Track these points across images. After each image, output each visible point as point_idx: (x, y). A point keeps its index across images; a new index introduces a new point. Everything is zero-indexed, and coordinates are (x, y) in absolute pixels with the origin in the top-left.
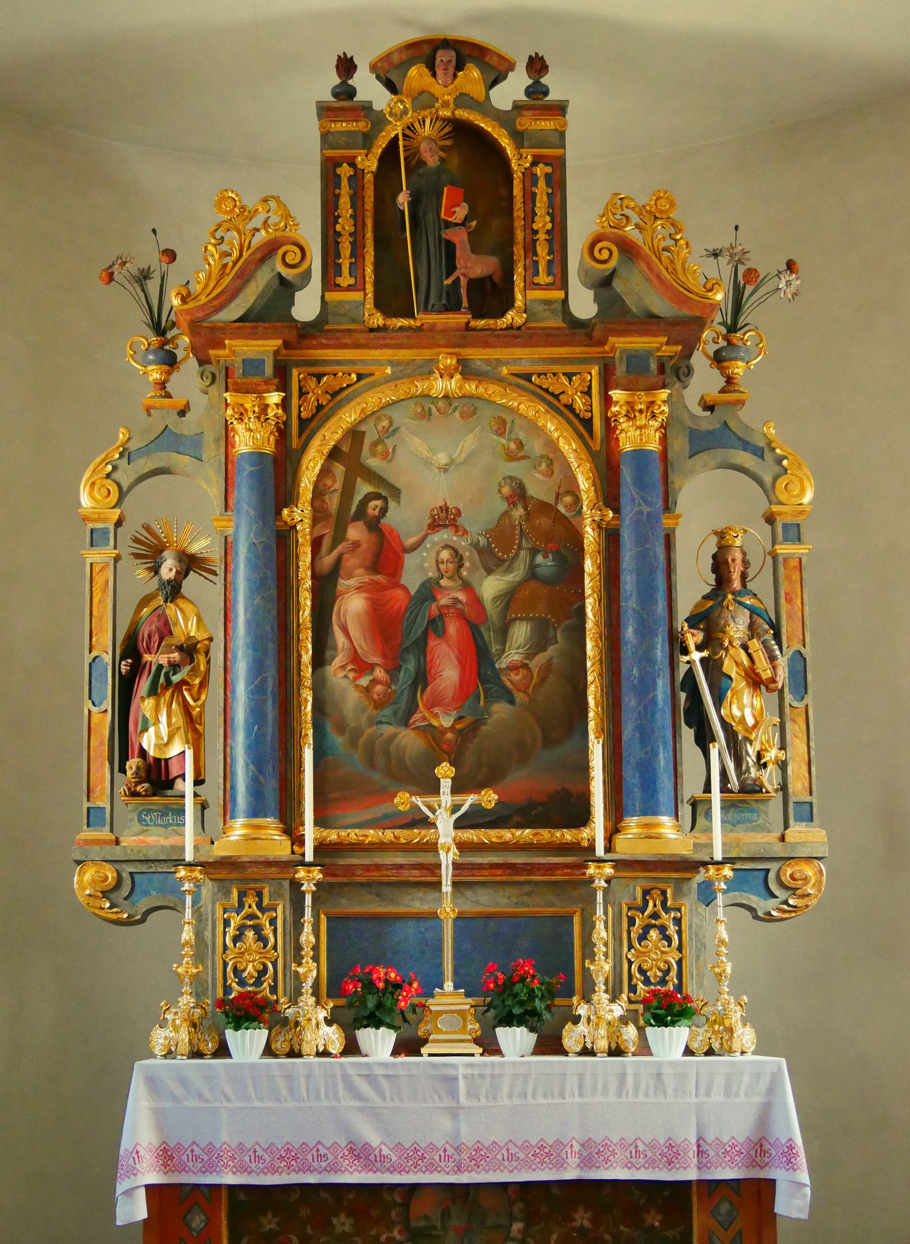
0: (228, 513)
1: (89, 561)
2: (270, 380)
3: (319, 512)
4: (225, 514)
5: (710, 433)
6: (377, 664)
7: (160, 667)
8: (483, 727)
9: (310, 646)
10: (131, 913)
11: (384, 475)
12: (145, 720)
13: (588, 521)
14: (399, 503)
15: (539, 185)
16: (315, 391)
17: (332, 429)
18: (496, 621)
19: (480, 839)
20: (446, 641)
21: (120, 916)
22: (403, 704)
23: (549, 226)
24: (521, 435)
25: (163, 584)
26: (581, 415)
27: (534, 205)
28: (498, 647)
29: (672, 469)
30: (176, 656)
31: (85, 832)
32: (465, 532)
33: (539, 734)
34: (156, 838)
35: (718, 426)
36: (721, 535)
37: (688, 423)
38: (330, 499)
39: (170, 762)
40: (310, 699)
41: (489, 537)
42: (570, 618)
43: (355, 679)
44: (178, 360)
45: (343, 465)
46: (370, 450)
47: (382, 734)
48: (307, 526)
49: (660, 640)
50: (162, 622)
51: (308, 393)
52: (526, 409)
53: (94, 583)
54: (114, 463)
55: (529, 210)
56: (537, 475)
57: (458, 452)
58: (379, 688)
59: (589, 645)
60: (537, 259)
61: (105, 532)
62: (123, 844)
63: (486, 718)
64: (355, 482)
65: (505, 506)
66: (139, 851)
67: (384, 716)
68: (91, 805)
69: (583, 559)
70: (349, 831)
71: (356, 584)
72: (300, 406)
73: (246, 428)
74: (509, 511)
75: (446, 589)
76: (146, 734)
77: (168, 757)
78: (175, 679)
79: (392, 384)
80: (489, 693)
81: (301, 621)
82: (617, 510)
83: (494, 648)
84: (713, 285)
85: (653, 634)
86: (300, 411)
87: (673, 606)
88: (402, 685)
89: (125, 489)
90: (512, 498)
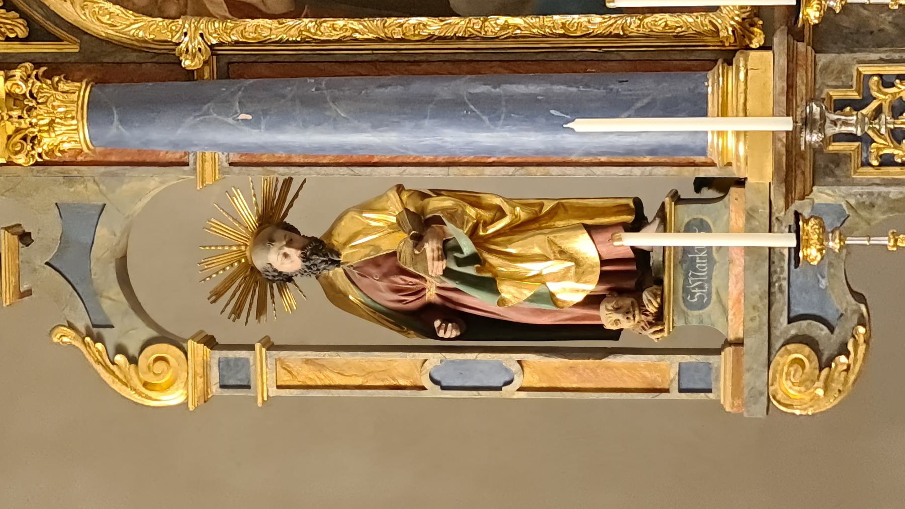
0: (191, 162)
1: (274, 392)
3: (186, 5)
7: (448, 273)
9: (414, 20)
10: (856, 322)
12: (536, 298)
21: (861, 340)
25: (309, 268)
30: (431, 247)
31: (719, 396)
34: (732, 280)
39: (605, 257)
40: (502, 20)
48: (211, 27)
50: (374, 271)
53: (310, 383)
54: (111, 351)
61: (224, 365)
62: (741, 335)
66: (754, 308)
68: (675, 386)
73: (48, 131)
76: (558, 296)
77: (597, 260)
78: (468, 248)
81: (371, 36)
86: (16, 39)
89: (153, 333)
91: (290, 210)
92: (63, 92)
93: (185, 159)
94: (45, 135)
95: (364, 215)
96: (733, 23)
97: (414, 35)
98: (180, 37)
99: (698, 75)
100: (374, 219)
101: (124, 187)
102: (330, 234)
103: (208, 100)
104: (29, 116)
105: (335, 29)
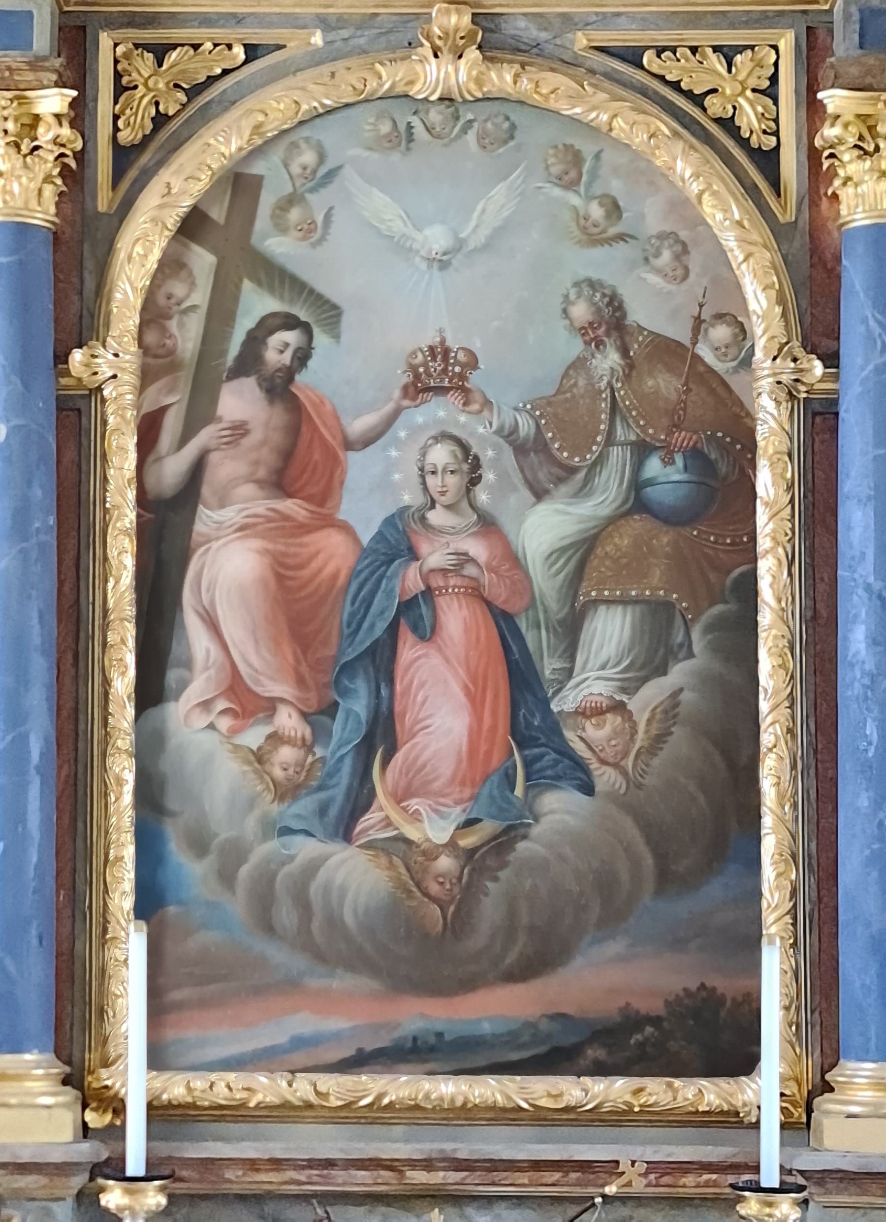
2: (45, 59)
3: (156, 356)
6: (282, 700)
8: (521, 846)
9: (130, 659)
11: (305, 275)
13: (766, 383)
14: (337, 337)
16: (151, 83)
17: (187, 172)
18: (553, 606)
19: (509, 1098)
20: (440, 650)
22: (338, 792)
24: (616, 187)
26: (754, 142)
32: (487, 403)
33: (648, 860)
38: (181, 325)
40: (130, 777)
41: (541, 416)
42: (726, 602)
43: (234, 731)
45: (214, 250)
46: (273, 216)
47: (292, 858)
51: (136, 87)
52: (626, 127)
56: (653, 279)
57: (473, 224)
58: (287, 754)
59: (766, 664)
63: (529, 825)
64: (238, 287)
65: (576, 347)
67: (298, 816)
69: (753, 464)
70: (213, 1076)
72: (116, 118)
74: (586, 359)
75: (440, 531)
79: (326, 69)
80: (538, 766)
81: (111, 603)
82: (831, 360)
86: (116, 129)
88: (340, 747)
90: (594, 329)
92: (40, 191)
96: (118, 1085)
97: (110, 660)
98: (113, 348)
99: (50, 1041)
103: (26, 385)
104: (7, 144)
105: (119, 554)
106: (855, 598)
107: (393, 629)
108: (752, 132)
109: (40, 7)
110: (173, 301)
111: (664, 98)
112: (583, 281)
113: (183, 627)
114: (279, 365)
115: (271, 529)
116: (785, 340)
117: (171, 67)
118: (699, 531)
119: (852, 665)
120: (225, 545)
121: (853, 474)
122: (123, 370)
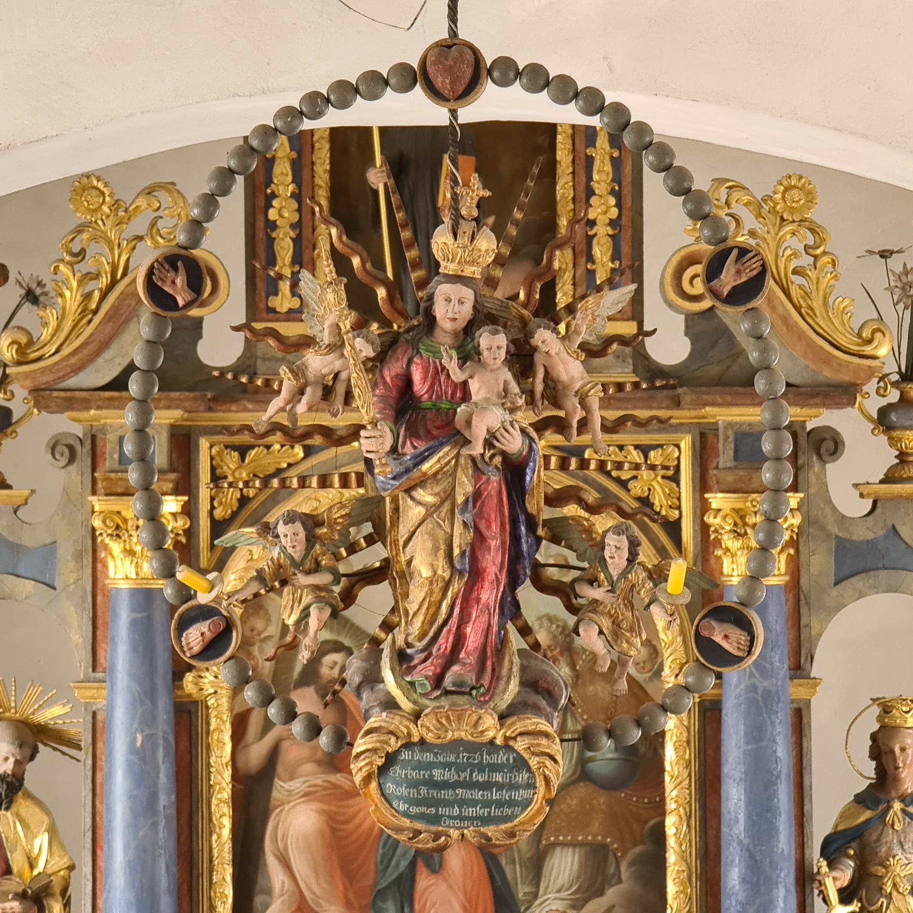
4: (93, 675)
5: (870, 544)
9: (229, 891)
15: (598, 144)
20: (445, 879)
23: (614, 213)
27: (590, 178)
28: (528, 889)
29: (808, 604)
35: (881, 533)
36: (886, 709)
37: (834, 530)
42: (643, 843)
44: (14, 420)
48: (224, 700)
49: (782, 892)
55: (581, 187)
59: (672, 889)
60: (594, 267)
71: (302, 788)
72: (212, 499)
81: (215, 853)
83: (522, 891)
84: (874, 332)
85: (771, 883)
86: (213, 508)
87: (806, 824)
90: (552, 650)
91: (50, 749)
93: (100, 668)
94: (122, 545)
95: (46, 834)
97: (215, 893)
100: (42, 841)
101: (72, 609)
102: (29, 796)
106: (732, 849)
107: (412, 865)
108: (661, 507)
109: (159, 433)
110: (255, 632)
111: (600, 485)
112: (543, 617)
113: (266, 865)
114: (330, 678)
115: (327, 795)
116: (684, 661)
117: (249, 463)
118: (626, 794)
119: (730, 896)
120: (293, 807)
121: (730, 760)
122: (222, 688)
